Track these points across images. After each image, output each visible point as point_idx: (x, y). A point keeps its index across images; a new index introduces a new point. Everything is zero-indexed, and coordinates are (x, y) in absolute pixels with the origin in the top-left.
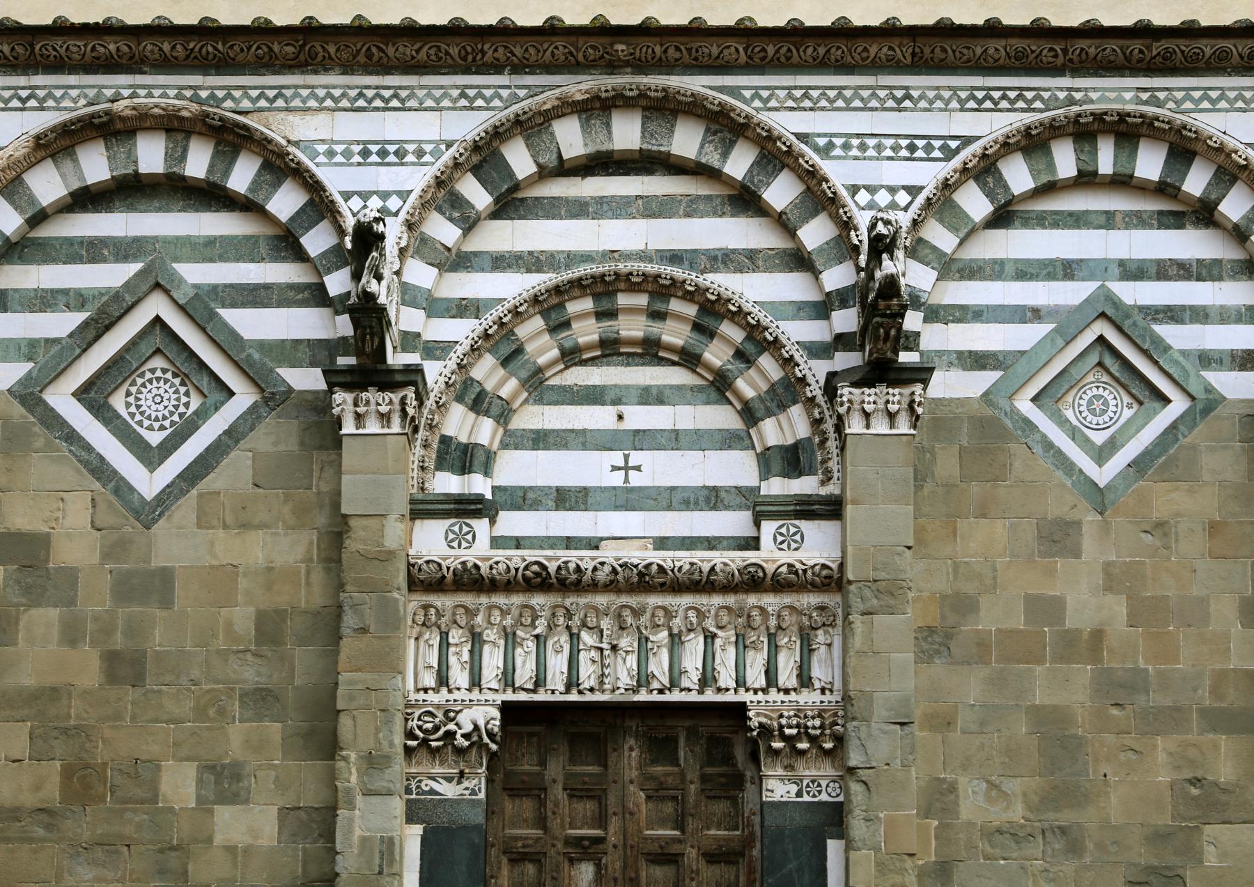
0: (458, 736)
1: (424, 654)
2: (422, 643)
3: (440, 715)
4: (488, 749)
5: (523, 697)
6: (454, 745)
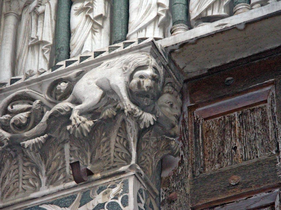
0: (75, 114)
1: (28, 31)
2: (25, 18)
3: (43, 96)
4: (138, 120)
5: (204, 29)
6: (72, 137)
